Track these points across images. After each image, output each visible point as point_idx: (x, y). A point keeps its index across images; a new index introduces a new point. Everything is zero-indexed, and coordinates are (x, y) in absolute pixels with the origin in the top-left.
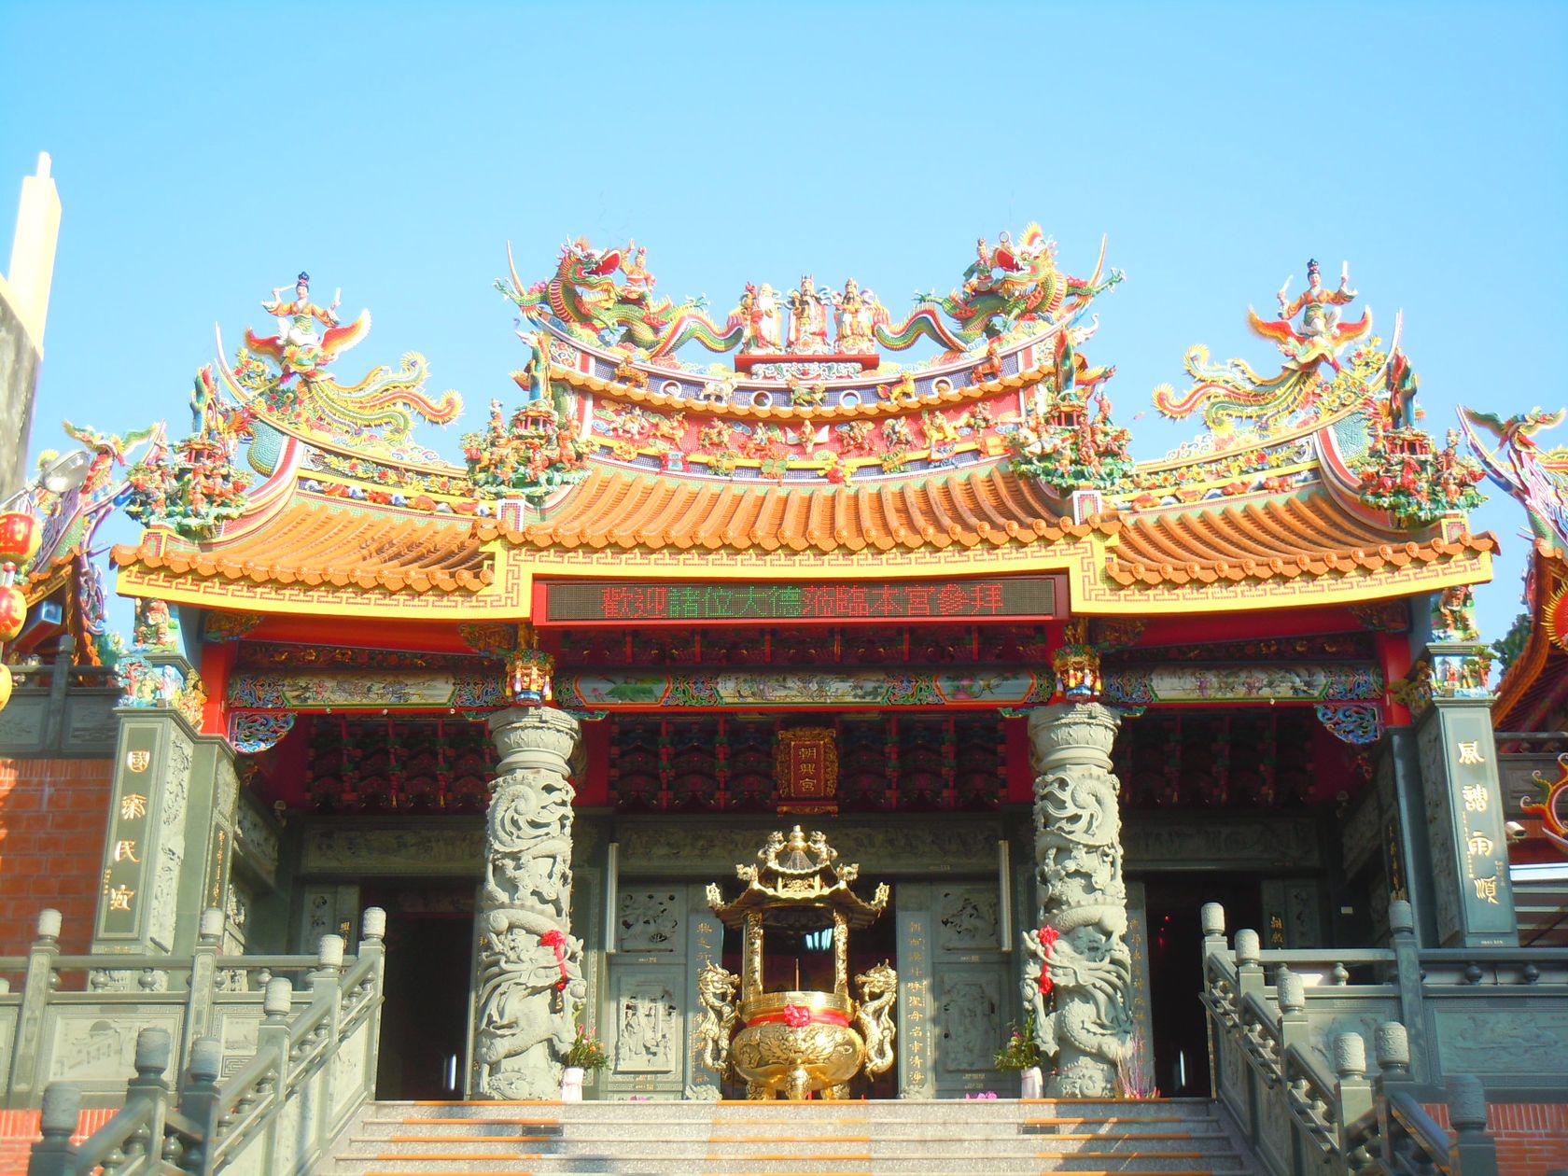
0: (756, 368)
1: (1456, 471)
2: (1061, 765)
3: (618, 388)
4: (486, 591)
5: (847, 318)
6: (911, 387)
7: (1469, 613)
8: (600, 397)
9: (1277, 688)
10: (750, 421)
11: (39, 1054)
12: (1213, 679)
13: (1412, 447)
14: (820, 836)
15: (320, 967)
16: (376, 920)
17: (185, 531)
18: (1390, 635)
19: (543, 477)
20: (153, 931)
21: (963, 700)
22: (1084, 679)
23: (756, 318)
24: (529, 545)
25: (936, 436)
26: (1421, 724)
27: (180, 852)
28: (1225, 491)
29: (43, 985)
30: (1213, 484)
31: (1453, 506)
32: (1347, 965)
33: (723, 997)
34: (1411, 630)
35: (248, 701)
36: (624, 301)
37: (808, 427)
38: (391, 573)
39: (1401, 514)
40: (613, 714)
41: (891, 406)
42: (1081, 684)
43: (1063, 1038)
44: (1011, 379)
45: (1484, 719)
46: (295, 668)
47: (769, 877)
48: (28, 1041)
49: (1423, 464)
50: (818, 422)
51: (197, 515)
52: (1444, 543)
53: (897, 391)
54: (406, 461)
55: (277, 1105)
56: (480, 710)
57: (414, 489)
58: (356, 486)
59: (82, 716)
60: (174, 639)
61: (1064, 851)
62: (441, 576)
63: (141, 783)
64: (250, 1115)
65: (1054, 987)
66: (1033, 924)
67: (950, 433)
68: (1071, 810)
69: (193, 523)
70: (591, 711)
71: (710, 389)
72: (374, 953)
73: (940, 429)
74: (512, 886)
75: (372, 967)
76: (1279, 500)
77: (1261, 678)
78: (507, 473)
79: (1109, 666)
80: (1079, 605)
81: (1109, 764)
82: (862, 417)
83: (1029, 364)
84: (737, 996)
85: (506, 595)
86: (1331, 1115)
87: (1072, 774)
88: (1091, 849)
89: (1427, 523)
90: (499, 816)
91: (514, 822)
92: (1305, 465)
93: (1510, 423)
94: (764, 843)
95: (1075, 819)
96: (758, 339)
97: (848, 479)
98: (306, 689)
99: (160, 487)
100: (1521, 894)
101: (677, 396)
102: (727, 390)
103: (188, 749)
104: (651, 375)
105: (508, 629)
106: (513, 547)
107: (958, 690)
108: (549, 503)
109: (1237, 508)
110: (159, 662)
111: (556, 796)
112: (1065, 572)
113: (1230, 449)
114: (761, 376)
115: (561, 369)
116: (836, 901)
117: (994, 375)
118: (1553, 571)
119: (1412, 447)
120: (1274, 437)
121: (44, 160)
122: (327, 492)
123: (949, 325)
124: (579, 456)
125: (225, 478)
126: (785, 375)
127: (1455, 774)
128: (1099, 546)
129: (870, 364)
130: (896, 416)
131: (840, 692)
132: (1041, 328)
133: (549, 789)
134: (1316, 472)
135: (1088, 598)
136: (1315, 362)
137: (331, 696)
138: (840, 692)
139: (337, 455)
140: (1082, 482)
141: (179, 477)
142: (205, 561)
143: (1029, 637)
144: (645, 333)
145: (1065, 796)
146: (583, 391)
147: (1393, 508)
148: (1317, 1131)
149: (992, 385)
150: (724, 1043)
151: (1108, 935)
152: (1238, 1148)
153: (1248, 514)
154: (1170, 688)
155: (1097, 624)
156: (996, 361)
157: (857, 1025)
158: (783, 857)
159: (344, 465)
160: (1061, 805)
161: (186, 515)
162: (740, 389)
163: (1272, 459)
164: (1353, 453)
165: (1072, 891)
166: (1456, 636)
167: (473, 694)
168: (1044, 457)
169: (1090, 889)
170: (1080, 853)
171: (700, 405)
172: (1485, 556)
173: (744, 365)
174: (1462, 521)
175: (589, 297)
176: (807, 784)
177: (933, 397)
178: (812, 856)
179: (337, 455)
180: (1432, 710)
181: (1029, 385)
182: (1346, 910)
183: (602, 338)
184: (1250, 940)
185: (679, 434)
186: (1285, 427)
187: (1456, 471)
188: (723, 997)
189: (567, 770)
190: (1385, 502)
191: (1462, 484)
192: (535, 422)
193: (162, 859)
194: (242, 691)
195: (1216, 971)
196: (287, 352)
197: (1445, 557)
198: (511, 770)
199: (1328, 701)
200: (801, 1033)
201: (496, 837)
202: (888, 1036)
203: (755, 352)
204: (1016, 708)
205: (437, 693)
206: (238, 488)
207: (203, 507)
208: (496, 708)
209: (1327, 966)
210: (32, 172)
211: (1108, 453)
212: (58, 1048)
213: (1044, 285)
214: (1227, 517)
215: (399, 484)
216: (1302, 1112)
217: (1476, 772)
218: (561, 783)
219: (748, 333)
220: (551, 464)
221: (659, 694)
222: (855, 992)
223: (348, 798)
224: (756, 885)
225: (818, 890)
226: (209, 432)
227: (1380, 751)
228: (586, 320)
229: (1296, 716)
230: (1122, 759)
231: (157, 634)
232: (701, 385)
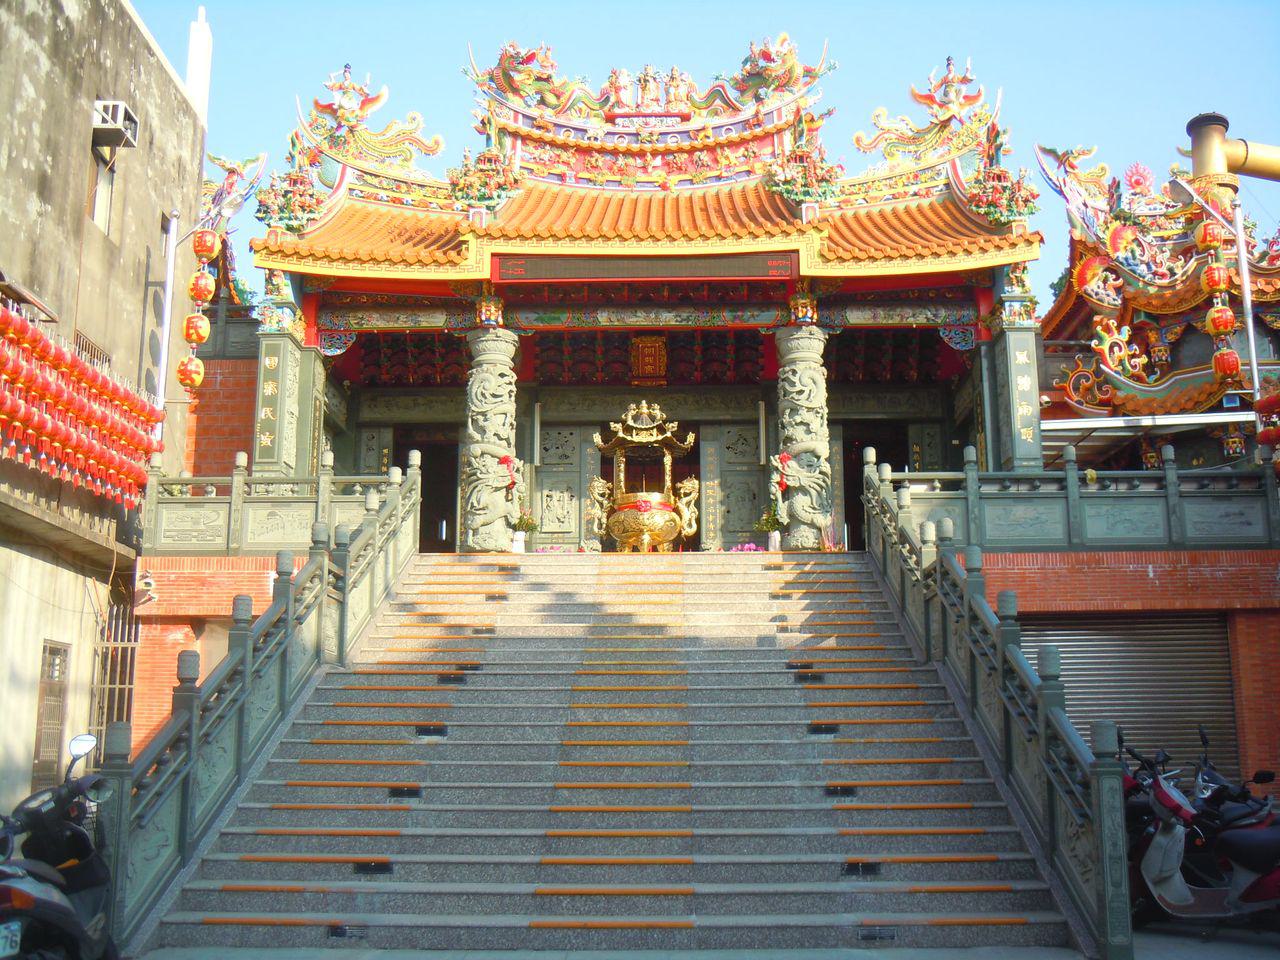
0: (618, 120)
1: (1023, 193)
2: (793, 362)
3: (536, 133)
4: (465, 262)
5: (672, 90)
6: (710, 132)
7: (1025, 277)
8: (525, 139)
9: (917, 318)
10: (615, 152)
11: (242, 528)
12: (881, 312)
13: (999, 178)
14: (657, 406)
15: (390, 484)
16: (415, 457)
17: (290, 228)
18: (981, 290)
19: (495, 194)
20: (285, 458)
22: (806, 312)
23: (617, 90)
24: (489, 236)
25: (724, 162)
26: (996, 340)
27: (296, 413)
28: (894, 197)
30: (887, 192)
31: (1020, 214)
32: (940, 480)
33: (602, 495)
34: (994, 285)
35: (329, 326)
36: (539, 79)
37: (649, 157)
38: (409, 252)
39: (991, 218)
40: (538, 332)
41: (698, 144)
42: (805, 316)
43: (792, 515)
44: (769, 127)
45: (1031, 338)
46: (356, 306)
47: (628, 429)
49: (1004, 189)
50: (655, 154)
51: (296, 218)
52: (1013, 237)
53: (702, 135)
54: (411, 179)
55: (375, 558)
57: (417, 195)
58: (383, 194)
59: (236, 335)
60: (288, 293)
61: (794, 410)
62: (439, 255)
63: (274, 375)
64: (363, 563)
65: (788, 487)
67: (733, 161)
68: (799, 387)
69: (295, 223)
70: (525, 330)
72: (415, 473)
73: (727, 158)
74: (482, 431)
75: (414, 483)
76: (925, 202)
77: (909, 312)
78: (474, 192)
79: (821, 305)
80: (805, 271)
81: (822, 361)
82: (681, 150)
83: (780, 117)
84: (611, 495)
85: (475, 265)
86: (918, 563)
87: (799, 367)
88: (810, 409)
89: (1005, 224)
90: (474, 391)
91: (483, 395)
92: (941, 181)
93: (1064, 155)
94: (626, 410)
95: (801, 392)
96: (619, 103)
97: (673, 188)
98: (362, 319)
99: (275, 203)
100: (1045, 436)
101: (572, 138)
102: (601, 135)
103: (298, 354)
104: (555, 125)
105: (477, 285)
106: (479, 237)
107: (735, 318)
108: (497, 209)
109: (901, 207)
110: (280, 305)
112: (797, 251)
113: (897, 172)
115: (502, 122)
116: (665, 443)
117: (759, 125)
118: (1080, 248)
119: (999, 178)
120: (923, 164)
121: (202, 11)
122: (366, 197)
123: (733, 94)
124: (516, 181)
125: (311, 196)
126: (635, 125)
129: (685, 118)
130: (701, 150)
131: (668, 319)
132: (787, 96)
133: (502, 375)
134: (948, 185)
135: (810, 267)
136: (949, 120)
137: (376, 322)
138: (668, 319)
139: (371, 174)
140: (808, 198)
141: (284, 196)
142: (303, 246)
143: (776, 288)
144: (551, 99)
145: (795, 379)
146: (515, 135)
147: (987, 214)
148: (911, 570)
149: (758, 131)
150: (604, 520)
151: (818, 458)
152: (877, 578)
153: (907, 211)
154: (857, 317)
155: (815, 281)
156: (761, 116)
157: (676, 510)
158: (636, 418)
159: (375, 181)
160: (793, 384)
161: (290, 219)
162: (609, 133)
164: (969, 174)
165: (798, 433)
167: (457, 321)
168: (786, 182)
169: (809, 432)
170: (803, 412)
171: (585, 143)
172: (1036, 245)
173: (611, 119)
174: (1024, 223)
175: (517, 77)
176: (649, 368)
177: (722, 139)
178: (653, 418)
179: (371, 174)
180: (1002, 333)
181: (780, 131)
183: (526, 103)
184: (887, 468)
185: (573, 161)
186: (930, 158)
187: (1023, 193)
188: (602, 495)
189: (512, 364)
190: (982, 211)
191: (1026, 201)
192: (490, 160)
193: (287, 417)
194: (326, 320)
195: (870, 485)
196: (339, 113)
197: (1013, 245)
198: (480, 364)
199: (946, 326)
200: (646, 515)
202: (694, 516)
203: (617, 111)
204: (768, 328)
205: (437, 321)
206: (319, 202)
207: (300, 214)
209: (931, 481)
210: (196, 20)
211: (823, 180)
212: (251, 526)
213: (790, 71)
214: (895, 212)
215: (408, 192)
216: (905, 561)
219: (613, 99)
220: (500, 186)
221: (564, 320)
222: (676, 492)
224: (621, 434)
225: (655, 437)
226: (300, 167)
227: (975, 353)
228: (516, 91)
229: (929, 333)
230: (829, 358)
232: (585, 131)
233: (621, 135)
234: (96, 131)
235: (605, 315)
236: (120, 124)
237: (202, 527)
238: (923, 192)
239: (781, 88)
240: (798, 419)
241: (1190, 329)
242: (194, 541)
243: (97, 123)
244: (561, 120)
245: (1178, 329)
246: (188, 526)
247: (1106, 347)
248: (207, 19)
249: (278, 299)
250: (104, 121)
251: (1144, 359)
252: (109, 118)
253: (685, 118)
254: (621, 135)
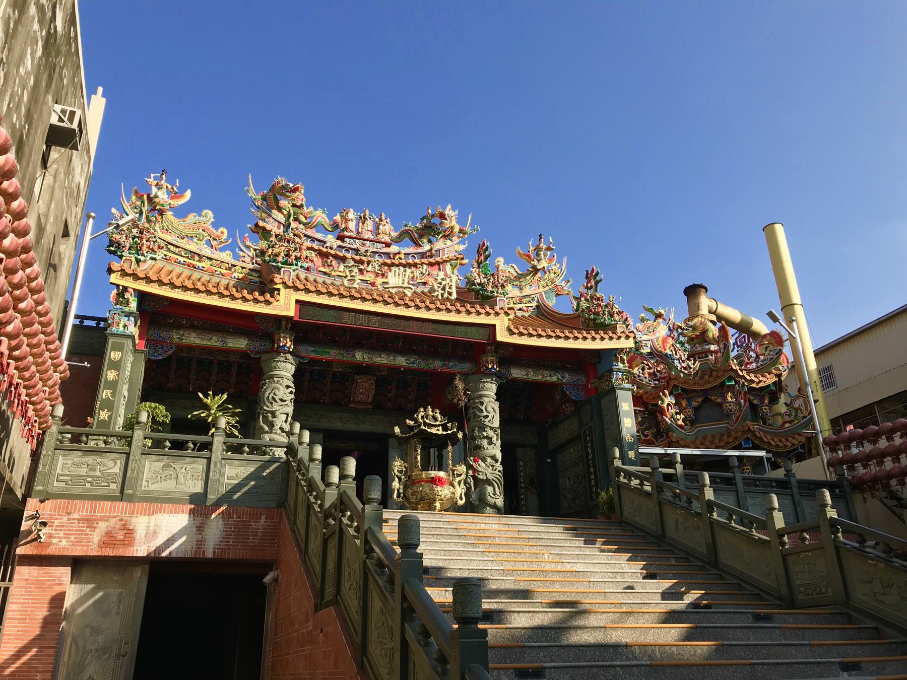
0: (346, 239)
2: (481, 396)
4: (275, 303)
6: (402, 256)
9: (552, 378)
14: (438, 411)
18: (599, 360)
21: (445, 370)
22: (493, 367)
23: (347, 221)
24: (296, 289)
29: (140, 444)
33: (401, 472)
48: (133, 470)
53: (397, 257)
54: (203, 253)
56: (257, 353)
57: (206, 264)
58: (182, 259)
66: (471, 455)
68: (485, 413)
70: (303, 358)
71: (328, 244)
74: (271, 425)
76: (526, 314)
77: (547, 373)
80: (499, 338)
81: (495, 397)
84: (406, 472)
88: (492, 428)
90: (267, 395)
91: (274, 399)
92: (534, 304)
94: (417, 412)
95: (487, 417)
96: (346, 229)
98: (183, 335)
102: (335, 246)
105: (278, 320)
107: (444, 365)
110: (128, 315)
111: (290, 389)
112: (494, 326)
114: (348, 243)
120: (524, 294)
126: (357, 244)
127: (621, 414)
128: (506, 318)
132: (449, 242)
133: (288, 387)
135: (502, 336)
137: (193, 339)
139: (173, 245)
143: (476, 349)
144: (302, 218)
145: (483, 408)
150: (401, 491)
154: (517, 373)
159: (177, 250)
160: (482, 411)
163: (524, 300)
165: (485, 442)
166: (621, 366)
167: (257, 345)
168: (479, 284)
169: (490, 442)
170: (488, 430)
173: (341, 238)
175: (284, 203)
176: (361, 397)
177: (410, 261)
179: (173, 245)
181: (445, 262)
182: (549, 460)
186: (527, 291)
188: (401, 472)
189: (292, 379)
190: (592, 317)
198: (272, 377)
199: (567, 384)
200: (439, 488)
201: (265, 404)
202: (464, 491)
203: (346, 233)
205: (241, 343)
208: (264, 352)
212: (146, 475)
215: (199, 261)
217: (627, 414)
218: (292, 385)
221: (332, 354)
223: (170, 385)
228: (280, 209)
231: (127, 303)
232: (325, 242)
233: (347, 250)
234: (52, 127)
235: (360, 354)
236: (75, 126)
237: (98, 474)
238: (525, 309)
239: (446, 237)
240: (485, 434)
241: (706, 400)
242: (88, 485)
243: (54, 120)
244: (309, 232)
245: (700, 400)
246: (83, 471)
247: (665, 405)
248: (103, 96)
249: (127, 309)
250: (61, 120)
251: (682, 416)
252: (66, 119)
253: (388, 245)
254: (347, 250)
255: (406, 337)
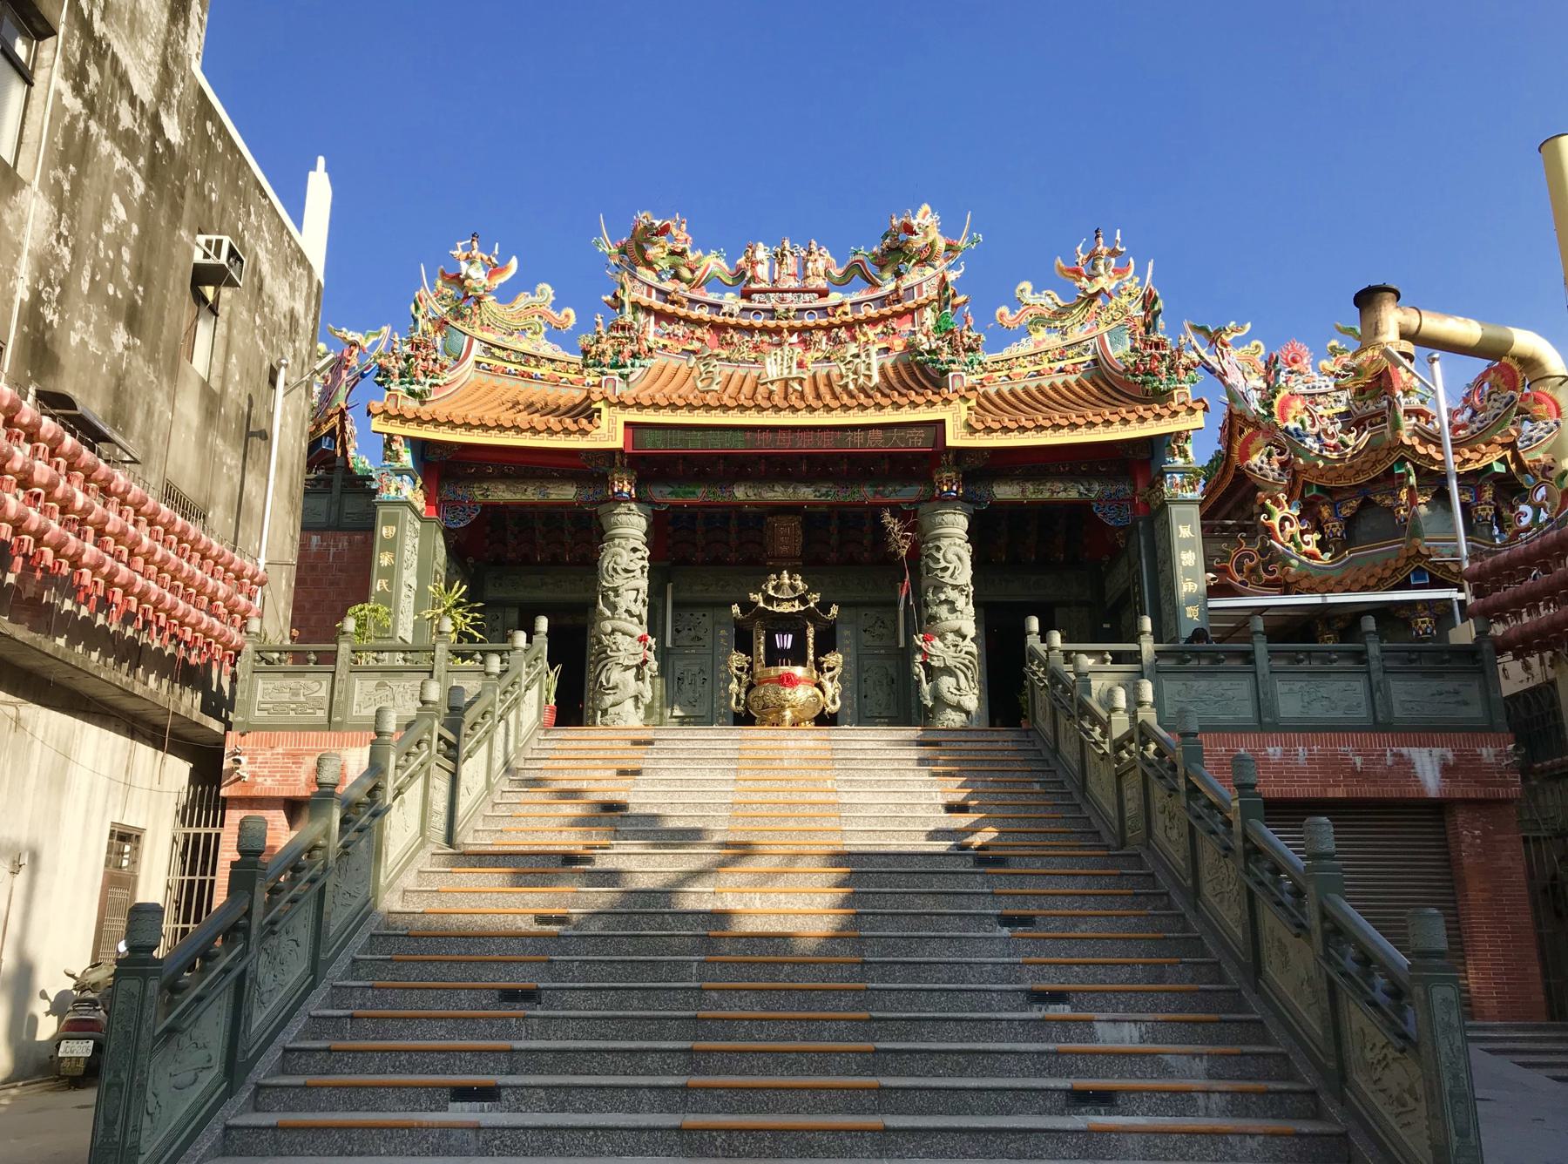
1: (1184, 360)
3: (669, 308)
5: (810, 265)
6: (848, 308)
7: (1189, 447)
8: (661, 316)
9: (1070, 492)
10: (750, 330)
11: (347, 698)
12: (1030, 487)
13: (1157, 346)
14: (798, 577)
15: (515, 649)
16: (543, 624)
17: (412, 393)
19: (629, 362)
20: (401, 633)
23: (754, 264)
24: (622, 405)
25: (863, 339)
26: (1156, 516)
27: (415, 586)
28: (1039, 373)
30: (1032, 369)
31: (1181, 382)
32: (1111, 653)
33: (741, 669)
34: (1153, 457)
35: (452, 497)
36: (672, 253)
37: (786, 333)
39: (1149, 387)
40: (673, 506)
41: (836, 321)
42: (950, 490)
43: (937, 696)
44: (910, 304)
45: (1195, 511)
46: (481, 477)
47: (769, 600)
49: (1163, 356)
50: (792, 330)
51: (418, 383)
52: (1174, 405)
53: (840, 311)
54: (541, 353)
55: (494, 727)
56: (593, 503)
57: (546, 370)
58: (511, 367)
59: (352, 505)
60: (407, 459)
61: (939, 587)
62: (568, 422)
63: (392, 545)
64: (480, 732)
65: (932, 667)
67: (871, 336)
68: (943, 564)
69: (417, 388)
70: (658, 504)
71: (726, 309)
72: (542, 642)
73: (865, 334)
74: (613, 607)
75: (541, 651)
76: (1072, 379)
77: (1059, 486)
78: (607, 360)
79: (968, 478)
80: (951, 442)
82: (818, 327)
83: (920, 294)
85: (609, 433)
86: (1104, 734)
87: (944, 543)
88: (955, 587)
89: (1165, 392)
91: (615, 570)
92: (1088, 357)
93: (1216, 332)
94: (766, 581)
95: (945, 569)
96: (754, 278)
97: (810, 366)
99: (396, 366)
100: (1212, 614)
101: (704, 313)
102: (736, 311)
103: (418, 525)
104: (690, 300)
106: (611, 405)
107: (876, 493)
108: (632, 378)
109: (1046, 384)
110: (400, 473)
111: (639, 554)
112: (943, 422)
113: (1043, 347)
114: (757, 301)
115: (635, 296)
116: (808, 614)
117: (899, 301)
118: (1239, 423)
119: (1157, 346)
120: (1070, 339)
122: (491, 370)
123: (871, 269)
124: (650, 350)
125: (435, 361)
126: (772, 301)
128: (964, 407)
129: (823, 294)
130: (839, 327)
131: (806, 493)
132: (929, 271)
133: (635, 550)
134: (1095, 361)
135: (955, 438)
136: (1097, 293)
137: (502, 494)
138: (806, 493)
140: (953, 367)
141: (406, 360)
142: (425, 412)
143: (919, 463)
144: (686, 273)
145: (940, 556)
146: (648, 310)
147: (1144, 383)
148: (1096, 743)
149: (898, 307)
150: (743, 696)
151: (964, 637)
152: (1046, 755)
153: (1053, 387)
154: (1005, 492)
155: (961, 452)
156: (901, 292)
157: (819, 686)
158: (777, 588)
159: (503, 354)
160: (937, 561)
161: (411, 383)
162: (743, 310)
163: (1070, 353)
164: (1120, 352)
165: (943, 611)
166: (1180, 461)
168: (929, 352)
169: (953, 610)
170: (948, 590)
171: (720, 319)
172: (1200, 414)
173: (747, 295)
174: (1184, 391)
175: (652, 252)
178: (793, 588)
180: (1164, 506)
181: (921, 307)
183: (659, 276)
184: (1056, 638)
185: (707, 337)
186: (1076, 334)
187: (1184, 360)
188: (741, 669)
191: (1187, 369)
192: (623, 328)
193: (405, 590)
194: (447, 492)
195: (1034, 654)
196: (467, 283)
197: (1175, 413)
198: (612, 539)
199: (1099, 500)
200: (788, 690)
203: (753, 286)
204: (911, 504)
205: (566, 493)
206: (443, 368)
207: (422, 379)
208: (602, 502)
209: (1102, 652)
211: (970, 349)
213: (932, 245)
214: (1040, 389)
215: (537, 366)
216: (1087, 733)
217: (1187, 544)
218: (642, 547)
219: (749, 274)
220: (634, 355)
221: (699, 495)
222: (819, 667)
223: (511, 555)
224: (762, 604)
225: (798, 607)
226: (424, 332)
227: (1130, 531)
228: (649, 265)
229: (1079, 509)
230: (973, 535)
231: (397, 457)
232: (720, 307)
233: (757, 312)
234: (197, 267)
235: (742, 489)
236: (223, 260)
237: (302, 699)
238: (1070, 368)
239: (923, 262)
240: (943, 597)
241: (1367, 503)
242: (292, 714)
243: (198, 257)
244: (696, 295)
245: (1354, 504)
246: (286, 697)
247: (1276, 522)
248: (327, 169)
249: (397, 465)
250: (206, 256)
251: (1317, 536)
252: (211, 253)
253: (823, 294)
254: (757, 312)
255: (810, 457)
